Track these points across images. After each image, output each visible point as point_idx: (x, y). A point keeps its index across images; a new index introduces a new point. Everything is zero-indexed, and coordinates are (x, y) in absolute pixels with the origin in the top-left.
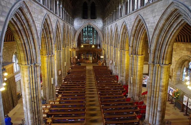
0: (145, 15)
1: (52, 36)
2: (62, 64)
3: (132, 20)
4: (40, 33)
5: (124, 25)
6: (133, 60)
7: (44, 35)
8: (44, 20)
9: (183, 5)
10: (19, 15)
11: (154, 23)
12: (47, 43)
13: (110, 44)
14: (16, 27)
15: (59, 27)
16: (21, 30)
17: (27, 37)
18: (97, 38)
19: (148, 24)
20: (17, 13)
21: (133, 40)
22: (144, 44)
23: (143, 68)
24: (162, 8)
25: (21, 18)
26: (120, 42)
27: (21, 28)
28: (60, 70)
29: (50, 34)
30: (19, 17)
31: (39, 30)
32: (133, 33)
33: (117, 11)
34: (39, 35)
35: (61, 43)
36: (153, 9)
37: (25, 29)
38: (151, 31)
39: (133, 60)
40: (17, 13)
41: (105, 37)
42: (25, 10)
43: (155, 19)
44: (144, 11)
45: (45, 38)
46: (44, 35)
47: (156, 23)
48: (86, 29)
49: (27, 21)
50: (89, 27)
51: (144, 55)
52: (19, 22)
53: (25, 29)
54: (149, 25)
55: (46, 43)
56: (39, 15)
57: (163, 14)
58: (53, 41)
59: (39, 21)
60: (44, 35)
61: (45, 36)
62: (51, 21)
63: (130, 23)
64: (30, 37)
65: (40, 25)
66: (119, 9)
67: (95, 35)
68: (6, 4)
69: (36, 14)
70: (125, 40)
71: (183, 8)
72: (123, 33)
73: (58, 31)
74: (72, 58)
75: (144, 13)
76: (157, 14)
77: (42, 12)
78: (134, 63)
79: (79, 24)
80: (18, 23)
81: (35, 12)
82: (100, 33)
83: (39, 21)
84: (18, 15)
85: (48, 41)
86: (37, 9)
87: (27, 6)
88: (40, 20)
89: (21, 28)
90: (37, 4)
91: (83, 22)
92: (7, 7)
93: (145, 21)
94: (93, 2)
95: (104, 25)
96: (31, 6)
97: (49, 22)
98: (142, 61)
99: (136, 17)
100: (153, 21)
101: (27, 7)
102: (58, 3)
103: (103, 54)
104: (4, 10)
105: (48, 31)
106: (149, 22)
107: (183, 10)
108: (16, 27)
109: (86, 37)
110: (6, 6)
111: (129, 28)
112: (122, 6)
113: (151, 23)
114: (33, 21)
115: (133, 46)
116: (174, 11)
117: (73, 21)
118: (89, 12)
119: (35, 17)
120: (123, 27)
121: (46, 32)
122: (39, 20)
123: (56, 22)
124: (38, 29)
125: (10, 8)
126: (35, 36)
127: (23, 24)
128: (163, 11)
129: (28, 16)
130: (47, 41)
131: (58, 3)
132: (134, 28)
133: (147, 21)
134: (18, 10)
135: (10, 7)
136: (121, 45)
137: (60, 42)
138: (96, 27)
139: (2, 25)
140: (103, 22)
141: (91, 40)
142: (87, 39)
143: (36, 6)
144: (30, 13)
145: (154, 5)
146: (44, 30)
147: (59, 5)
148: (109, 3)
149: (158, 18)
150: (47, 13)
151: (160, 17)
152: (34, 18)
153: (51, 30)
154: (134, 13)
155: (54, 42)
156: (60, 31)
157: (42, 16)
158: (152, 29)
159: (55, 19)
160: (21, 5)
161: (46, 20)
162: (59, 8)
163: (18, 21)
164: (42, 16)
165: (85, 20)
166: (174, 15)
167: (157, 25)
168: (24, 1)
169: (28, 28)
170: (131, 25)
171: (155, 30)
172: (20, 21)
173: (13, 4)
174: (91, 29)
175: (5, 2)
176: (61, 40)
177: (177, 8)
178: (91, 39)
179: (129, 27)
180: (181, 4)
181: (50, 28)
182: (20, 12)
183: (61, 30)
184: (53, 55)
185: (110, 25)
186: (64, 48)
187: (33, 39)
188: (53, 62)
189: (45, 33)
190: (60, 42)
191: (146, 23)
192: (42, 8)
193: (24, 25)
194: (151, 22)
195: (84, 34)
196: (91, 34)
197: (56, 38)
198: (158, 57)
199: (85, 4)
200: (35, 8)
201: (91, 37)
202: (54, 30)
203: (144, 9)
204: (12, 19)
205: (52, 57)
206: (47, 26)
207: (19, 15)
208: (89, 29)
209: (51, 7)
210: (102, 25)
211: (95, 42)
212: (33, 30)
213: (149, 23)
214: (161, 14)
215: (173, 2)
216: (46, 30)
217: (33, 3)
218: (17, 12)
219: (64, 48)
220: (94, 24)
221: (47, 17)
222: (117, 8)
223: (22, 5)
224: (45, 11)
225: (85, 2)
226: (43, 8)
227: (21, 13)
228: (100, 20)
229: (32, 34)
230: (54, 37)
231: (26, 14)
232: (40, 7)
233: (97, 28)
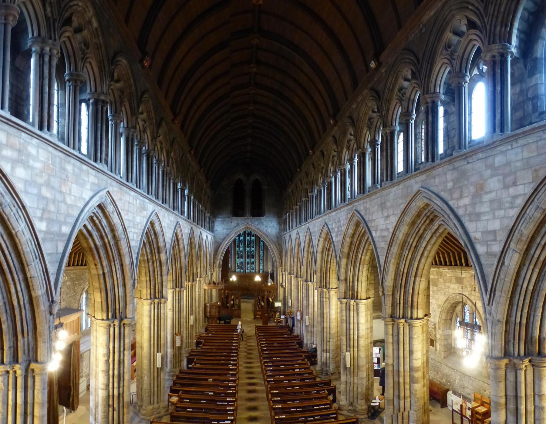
0: (368, 212)
1: (163, 257)
2: (183, 320)
3: (342, 222)
4: (137, 252)
5: (325, 231)
6: (348, 311)
7: (146, 256)
8: (149, 224)
9: (437, 198)
10: (97, 218)
11: (387, 229)
12: (151, 272)
13: (295, 274)
14: (90, 241)
15: (180, 236)
16: (99, 246)
17: (109, 261)
18: (267, 258)
19: (376, 233)
20: (93, 215)
21: (347, 265)
22: (371, 274)
23: (371, 328)
24: (400, 201)
25: (100, 222)
26: (318, 270)
27: (99, 243)
28: (180, 333)
29: (159, 252)
30: (97, 222)
31: (136, 246)
32: (346, 250)
33: (309, 200)
34: (134, 256)
35: (183, 271)
36: (383, 201)
37: (108, 245)
38: (383, 248)
39: (348, 311)
40: (93, 215)
41: (284, 258)
42: (110, 208)
43: (388, 222)
44: (365, 205)
45: (148, 262)
46: (147, 256)
47: (391, 231)
48: (242, 238)
49: (113, 230)
50: (248, 234)
51: (372, 299)
52: (97, 231)
53: (108, 245)
54: (378, 234)
55: (149, 272)
56: (137, 216)
57: (404, 213)
58: (164, 268)
59: (136, 227)
60: (147, 256)
61: (148, 259)
62: (163, 224)
63: (338, 228)
64: (116, 262)
65: (138, 237)
66: (315, 196)
67: (261, 253)
68: (75, 200)
69: (132, 214)
70: (329, 266)
71: (439, 202)
72: (323, 249)
73: (177, 247)
74: (208, 305)
75: (366, 209)
76: (391, 212)
77: (144, 208)
78: (352, 318)
79: (227, 229)
80: (95, 234)
81: (128, 211)
82: (272, 248)
83: (136, 227)
84: (95, 218)
85: (154, 267)
86: (133, 204)
87: (114, 201)
88: (140, 225)
89: (99, 243)
90: (135, 194)
91: (234, 224)
92: (76, 206)
93: (369, 225)
94: (257, 179)
95: (282, 230)
96: (121, 199)
97: (158, 228)
98: (369, 314)
99: (349, 216)
100: (384, 227)
101: (113, 202)
102: (179, 186)
103: (281, 297)
104: (70, 211)
105: (155, 246)
106: (377, 228)
107: (439, 206)
108: (90, 241)
109: (242, 257)
110: (73, 204)
111: (337, 240)
112: (321, 192)
113: (382, 230)
114: (125, 229)
115: (346, 280)
116: (423, 208)
117: (213, 222)
118: (248, 202)
119: (129, 220)
120: (323, 235)
121: (151, 250)
122: (138, 225)
123: (173, 228)
124: (133, 244)
125: (80, 207)
126: (127, 261)
127: (104, 234)
128: (403, 207)
129: (115, 219)
130: (151, 269)
131: (179, 186)
132: (348, 240)
133: (373, 224)
134: (96, 208)
135: (81, 205)
136: (321, 277)
137: (181, 269)
138: (264, 233)
139: (64, 240)
140: (279, 223)
141: (253, 263)
142: (242, 260)
143: (131, 198)
144: (120, 213)
145: (385, 192)
146: (147, 245)
147: (183, 190)
148: (292, 183)
149: (394, 220)
150: (154, 210)
151: (397, 218)
152: (127, 222)
153: (161, 244)
154: (346, 208)
155: (167, 271)
156: (181, 246)
157: (144, 217)
158: (383, 243)
159: (171, 221)
160: (102, 198)
161: (152, 224)
162: (183, 196)
163: (95, 230)
164: (144, 217)
165: (239, 218)
166: (424, 215)
167: (394, 234)
168: (108, 192)
169: (112, 243)
170: (339, 233)
171: (390, 245)
172: (98, 230)
173: (87, 199)
175: (73, 197)
176: (183, 265)
177: (429, 202)
178: (253, 260)
179: (337, 236)
180: (434, 196)
181: (161, 240)
182: (99, 211)
183: (183, 243)
184: (163, 300)
185: (295, 231)
186: (190, 284)
187: (122, 265)
188: (162, 315)
189: (148, 250)
190: (181, 269)
191: (371, 229)
192: (144, 201)
193: (105, 237)
194: (380, 227)
195: (237, 249)
196: (253, 249)
197: (173, 261)
198: (400, 303)
199: (239, 184)
200: (129, 203)
201: (253, 257)
202: (168, 246)
203: (365, 201)
204: (85, 226)
205: (162, 305)
206: (153, 237)
207: (97, 218)
208: (248, 238)
209: (165, 197)
210: (278, 230)
211: (261, 268)
212: (123, 247)
213: (376, 231)
214: (398, 212)
215: (419, 190)
216: (150, 245)
217: (126, 192)
218: (94, 213)
219: (190, 284)
220: (259, 227)
221: (153, 218)
222: (310, 194)
223: (104, 200)
224: (151, 207)
225: (239, 180)
226: (147, 201)
227: (101, 215)
228: (271, 219)
229: (120, 255)
230: (167, 260)
231: (112, 215)
232: (140, 200)
233: (267, 236)
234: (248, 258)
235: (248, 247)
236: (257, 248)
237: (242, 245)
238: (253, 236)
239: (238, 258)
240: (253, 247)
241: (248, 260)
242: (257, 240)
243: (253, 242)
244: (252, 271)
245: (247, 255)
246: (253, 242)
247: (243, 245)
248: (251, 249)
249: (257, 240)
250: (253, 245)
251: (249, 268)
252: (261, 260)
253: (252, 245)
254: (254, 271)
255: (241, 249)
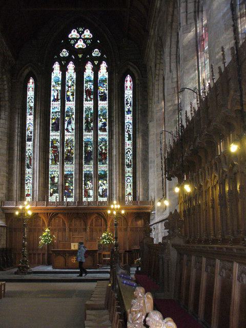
18: (146, 159)
48: (71, 105)
50: (89, 93)
67: (128, 144)
109: (69, 159)
141: (103, 177)
142: (70, 168)
174: (103, 105)
178: (103, 168)
195: (54, 135)
201: (100, 157)
208: (88, 104)
211: (129, 190)
234: (88, 161)
235: (88, 130)
236: (116, 130)
237: (69, 123)
238: (103, 99)
239: (55, 160)
240: (104, 130)
241: (88, 168)
242: (115, 107)
243: (104, 115)
244: (100, 199)
245: (86, 152)
246: (104, 115)
247: (73, 125)
248: (96, 136)
249: (115, 107)
250: (105, 124)
251: (91, 192)
252: (129, 166)
253: (100, 124)
254: (105, 199)
255: (70, 136)
